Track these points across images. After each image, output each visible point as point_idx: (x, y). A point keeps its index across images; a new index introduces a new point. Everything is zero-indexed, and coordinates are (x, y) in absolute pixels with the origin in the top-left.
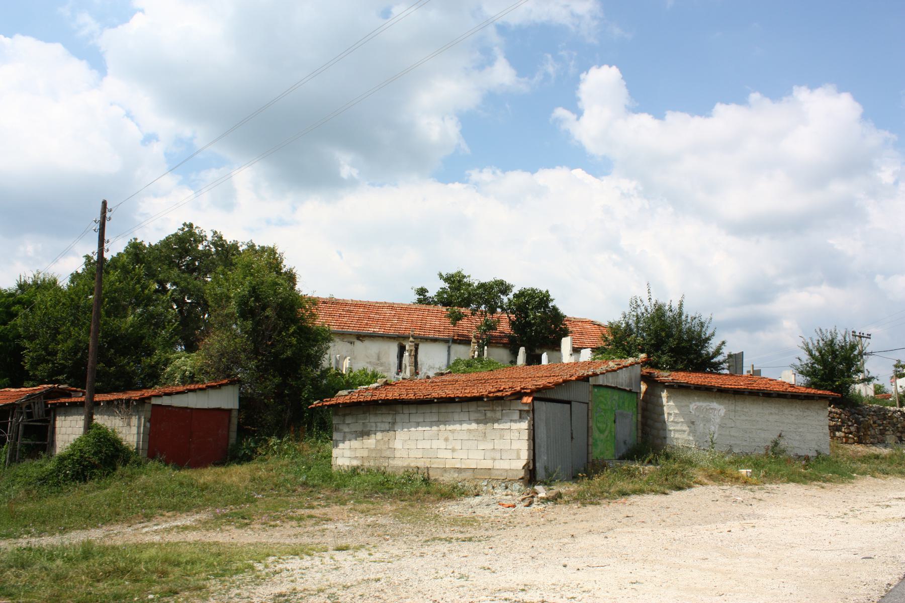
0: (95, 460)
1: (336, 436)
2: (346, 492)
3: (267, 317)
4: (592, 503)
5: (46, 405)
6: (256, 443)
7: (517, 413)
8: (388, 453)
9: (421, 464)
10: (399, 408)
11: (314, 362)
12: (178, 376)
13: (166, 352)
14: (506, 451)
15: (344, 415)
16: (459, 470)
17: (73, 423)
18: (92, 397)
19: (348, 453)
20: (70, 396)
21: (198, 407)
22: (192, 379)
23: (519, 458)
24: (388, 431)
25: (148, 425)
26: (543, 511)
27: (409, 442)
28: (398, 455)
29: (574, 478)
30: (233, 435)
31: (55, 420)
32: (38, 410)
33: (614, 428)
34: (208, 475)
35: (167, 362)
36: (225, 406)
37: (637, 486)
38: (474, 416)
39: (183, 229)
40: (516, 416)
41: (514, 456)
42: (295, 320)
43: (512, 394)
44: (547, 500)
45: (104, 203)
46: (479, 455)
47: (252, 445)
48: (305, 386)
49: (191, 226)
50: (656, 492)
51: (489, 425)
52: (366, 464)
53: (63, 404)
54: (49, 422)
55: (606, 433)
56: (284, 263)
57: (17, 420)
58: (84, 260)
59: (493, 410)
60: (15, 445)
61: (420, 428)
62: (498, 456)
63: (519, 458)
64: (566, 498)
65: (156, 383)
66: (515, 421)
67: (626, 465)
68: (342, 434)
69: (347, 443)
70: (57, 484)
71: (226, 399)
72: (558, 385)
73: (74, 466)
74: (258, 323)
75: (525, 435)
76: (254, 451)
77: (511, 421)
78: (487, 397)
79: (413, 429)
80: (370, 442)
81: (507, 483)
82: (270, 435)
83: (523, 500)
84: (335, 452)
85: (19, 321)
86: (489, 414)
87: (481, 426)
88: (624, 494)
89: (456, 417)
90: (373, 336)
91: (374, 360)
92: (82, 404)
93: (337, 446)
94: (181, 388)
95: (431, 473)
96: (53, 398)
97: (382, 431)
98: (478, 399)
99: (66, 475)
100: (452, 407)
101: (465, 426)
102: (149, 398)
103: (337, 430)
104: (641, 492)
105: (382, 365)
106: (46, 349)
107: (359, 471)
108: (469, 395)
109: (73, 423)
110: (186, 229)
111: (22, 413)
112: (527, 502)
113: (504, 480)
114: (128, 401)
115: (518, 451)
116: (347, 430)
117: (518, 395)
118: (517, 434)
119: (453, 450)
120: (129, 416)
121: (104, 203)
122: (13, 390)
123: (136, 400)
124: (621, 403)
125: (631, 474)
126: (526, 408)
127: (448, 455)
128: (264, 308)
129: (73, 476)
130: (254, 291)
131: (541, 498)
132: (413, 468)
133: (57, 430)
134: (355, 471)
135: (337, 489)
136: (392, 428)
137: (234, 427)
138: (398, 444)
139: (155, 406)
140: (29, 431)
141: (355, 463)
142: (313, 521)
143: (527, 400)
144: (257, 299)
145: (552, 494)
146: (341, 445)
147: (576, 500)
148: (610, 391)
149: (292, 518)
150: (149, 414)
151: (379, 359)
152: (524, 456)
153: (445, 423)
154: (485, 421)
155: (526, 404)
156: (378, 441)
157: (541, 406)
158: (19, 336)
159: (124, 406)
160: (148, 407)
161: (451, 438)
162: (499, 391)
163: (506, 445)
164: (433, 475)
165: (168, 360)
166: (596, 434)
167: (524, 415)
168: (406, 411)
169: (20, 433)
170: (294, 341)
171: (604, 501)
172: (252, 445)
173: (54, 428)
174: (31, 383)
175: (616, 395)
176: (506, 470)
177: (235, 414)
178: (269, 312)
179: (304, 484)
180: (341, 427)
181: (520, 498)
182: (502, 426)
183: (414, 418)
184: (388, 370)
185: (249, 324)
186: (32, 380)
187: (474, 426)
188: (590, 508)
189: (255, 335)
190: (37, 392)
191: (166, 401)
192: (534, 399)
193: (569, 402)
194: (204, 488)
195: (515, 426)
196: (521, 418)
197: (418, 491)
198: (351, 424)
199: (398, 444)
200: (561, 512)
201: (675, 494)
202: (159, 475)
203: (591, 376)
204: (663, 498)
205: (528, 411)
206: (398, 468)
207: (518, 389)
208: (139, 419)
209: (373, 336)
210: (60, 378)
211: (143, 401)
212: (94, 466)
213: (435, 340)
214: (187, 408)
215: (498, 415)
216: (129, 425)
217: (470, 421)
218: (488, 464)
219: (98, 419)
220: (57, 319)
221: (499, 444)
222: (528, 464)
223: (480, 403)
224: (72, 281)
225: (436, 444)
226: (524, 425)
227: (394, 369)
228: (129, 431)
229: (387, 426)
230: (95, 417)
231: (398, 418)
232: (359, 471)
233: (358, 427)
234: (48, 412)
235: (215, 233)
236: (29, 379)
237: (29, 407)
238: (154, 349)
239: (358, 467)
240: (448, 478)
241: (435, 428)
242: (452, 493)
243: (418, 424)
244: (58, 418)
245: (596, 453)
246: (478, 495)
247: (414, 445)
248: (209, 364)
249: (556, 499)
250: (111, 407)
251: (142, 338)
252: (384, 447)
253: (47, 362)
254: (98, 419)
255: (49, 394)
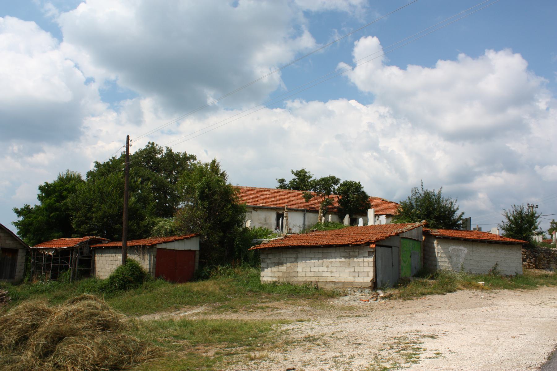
0: (131, 278)
1: (262, 265)
2: (275, 294)
3: (215, 200)
4: (409, 299)
5: (90, 248)
6: (211, 268)
7: (367, 253)
8: (294, 274)
9: (313, 280)
10: (300, 250)
11: (239, 223)
12: (163, 232)
13: (152, 218)
14: (361, 272)
15: (268, 254)
16: (335, 283)
17: (107, 258)
18: (126, 243)
19: (270, 274)
20: (101, 243)
21: (180, 249)
22: (172, 233)
23: (368, 276)
24: (293, 262)
25: (155, 259)
26: (385, 303)
27: (306, 268)
28: (299, 275)
29: (395, 286)
30: (197, 264)
31: (95, 256)
32: (86, 251)
33: (410, 261)
34: (196, 286)
35: (154, 224)
36: (192, 249)
37: (429, 291)
38: (343, 254)
39: (148, 146)
40: (367, 254)
41: (366, 275)
42: (229, 201)
43: (365, 243)
44: (385, 298)
45: (128, 137)
46: (346, 275)
47: (208, 270)
48: (236, 238)
49: (153, 144)
50: (439, 294)
51: (351, 259)
52: (281, 280)
53: (101, 248)
54: (91, 257)
55: (407, 263)
56: (220, 168)
57: (75, 256)
58: (94, 164)
59: (354, 251)
60: (74, 270)
61: (312, 261)
62: (357, 275)
63: (368, 276)
64: (394, 296)
65: (149, 236)
66: (366, 257)
67: (420, 280)
68: (266, 264)
69: (269, 269)
70: (111, 292)
71: (193, 245)
72: (387, 238)
73: (120, 282)
74: (210, 203)
75: (372, 264)
76: (209, 273)
77: (364, 257)
78: (351, 244)
79: (308, 261)
80: (283, 268)
81: (362, 289)
82: (218, 265)
83: (372, 298)
84: (262, 274)
85: (69, 200)
86: (351, 253)
87: (347, 260)
88: (423, 294)
89: (333, 255)
90: (262, 208)
91: (263, 222)
92: (120, 247)
93: (263, 270)
94: (166, 239)
95: (319, 284)
96: (93, 244)
97: (290, 262)
98: (347, 245)
99: (116, 286)
100: (330, 250)
101: (338, 260)
102: (155, 245)
103: (263, 262)
104: (431, 293)
105: (267, 224)
106: (85, 216)
107: (277, 284)
108: (341, 243)
109: (107, 258)
110: (150, 146)
111: (77, 252)
112: (375, 299)
113: (360, 288)
114: (144, 246)
115: (368, 273)
116: (269, 262)
117: (368, 244)
118: (367, 264)
119: (331, 272)
120: (144, 254)
121: (128, 137)
122: (67, 239)
123: (149, 246)
124: (423, 246)
125: (424, 285)
126: (372, 250)
127: (329, 275)
128: (213, 194)
129: (119, 287)
130: (208, 185)
131: (381, 297)
132: (309, 282)
133: (96, 262)
134: (274, 284)
135: (269, 293)
136: (296, 260)
137: (197, 260)
138: (299, 269)
139: (158, 249)
140: (81, 262)
141: (274, 279)
142: (270, 310)
143: (373, 246)
144: (209, 190)
145: (386, 294)
146: (266, 270)
147: (400, 297)
148: (408, 241)
149: (258, 308)
150: (155, 254)
151: (265, 221)
152: (371, 275)
153: (326, 258)
154: (349, 257)
155: (372, 248)
156: (287, 268)
157: (379, 249)
158: (68, 209)
159: (141, 249)
160: (155, 249)
161: (330, 266)
162: (357, 241)
163: (363, 269)
164: (320, 286)
165: (154, 222)
166: (402, 264)
167: (371, 254)
168: (304, 252)
169: (77, 263)
170: (230, 212)
171: (414, 298)
172: (208, 270)
173: (94, 260)
174: (76, 235)
175: (411, 243)
176: (361, 283)
177: (197, 253)
178: (216, 197)
179: (251, 291)
180: (265, 260)
181: (370, 297)
182: (358, 260)
183: (308, 256)
184: (271, 227)
185: (206, 203)
186: (76, 234)
187: (343, 260)
188: (409, 301)
189: (210, 210)
190: (85, 240)
191: (164, 246)
192: (376, 245)
193: (391, 247)
194: (198, 293)
195: (366, 260)
196: (369, 256)
197: (316, 294)
198: (272, 258)
199: (299, 269)
200: (392, 303)
201: (449, 295)
202: (165, 287)
203: (400, 233)
204: (443, 297)
205: (373, 252)
206: (300, 282)
207: (368, 240)
208: (150, 256)
209: (262, 208)
210: (94, 232)
211: (152, 246)
212: (130, 282)
213: (296, 210)
214: (174, 250)
215: (357, 254)
216: (144, 259)
217: (341, 257)
218: (351, 279)
219: (130, 257)
220: (92, 199)
221: (357, 269)
222: (373, 279)
223: (346, 248)
224: (88, 177)
225: (321, 269)
226: (371, 259)
227: (274, 227)
228: (145, 263)
229: (293, 260)
230: (128, 255)
231: (299, 255)
232: (277, 284)
233: (276, 260)
234: (91, 252)
235: (168, 148)
236: (75, 233)
237: (81, 249)
238: (145, 216)
239: (276, 282)
240: (328, 287)
241: (321, 261)
242: (333, 295)
243: (311, 259)
244: (96, 255)
245: (403, 274)
246: (346, 296)
247: (308, 270)
248: (162, 225)
249: (389, 297)
250: (135, 249)
251: (138, 210)
252: (291, 271)
253: (87, 223)
254: (130, 257)
255: (91, 242)
